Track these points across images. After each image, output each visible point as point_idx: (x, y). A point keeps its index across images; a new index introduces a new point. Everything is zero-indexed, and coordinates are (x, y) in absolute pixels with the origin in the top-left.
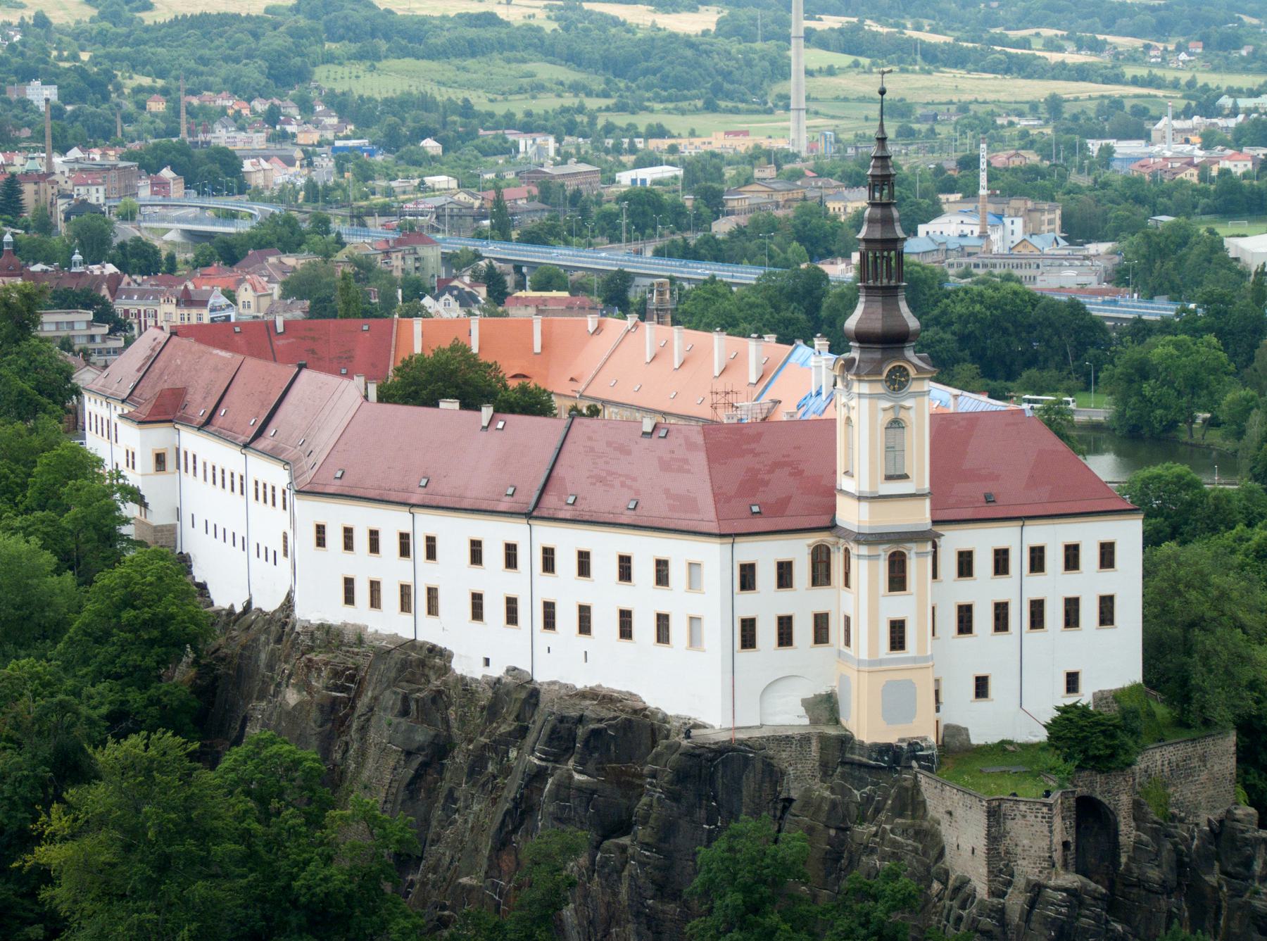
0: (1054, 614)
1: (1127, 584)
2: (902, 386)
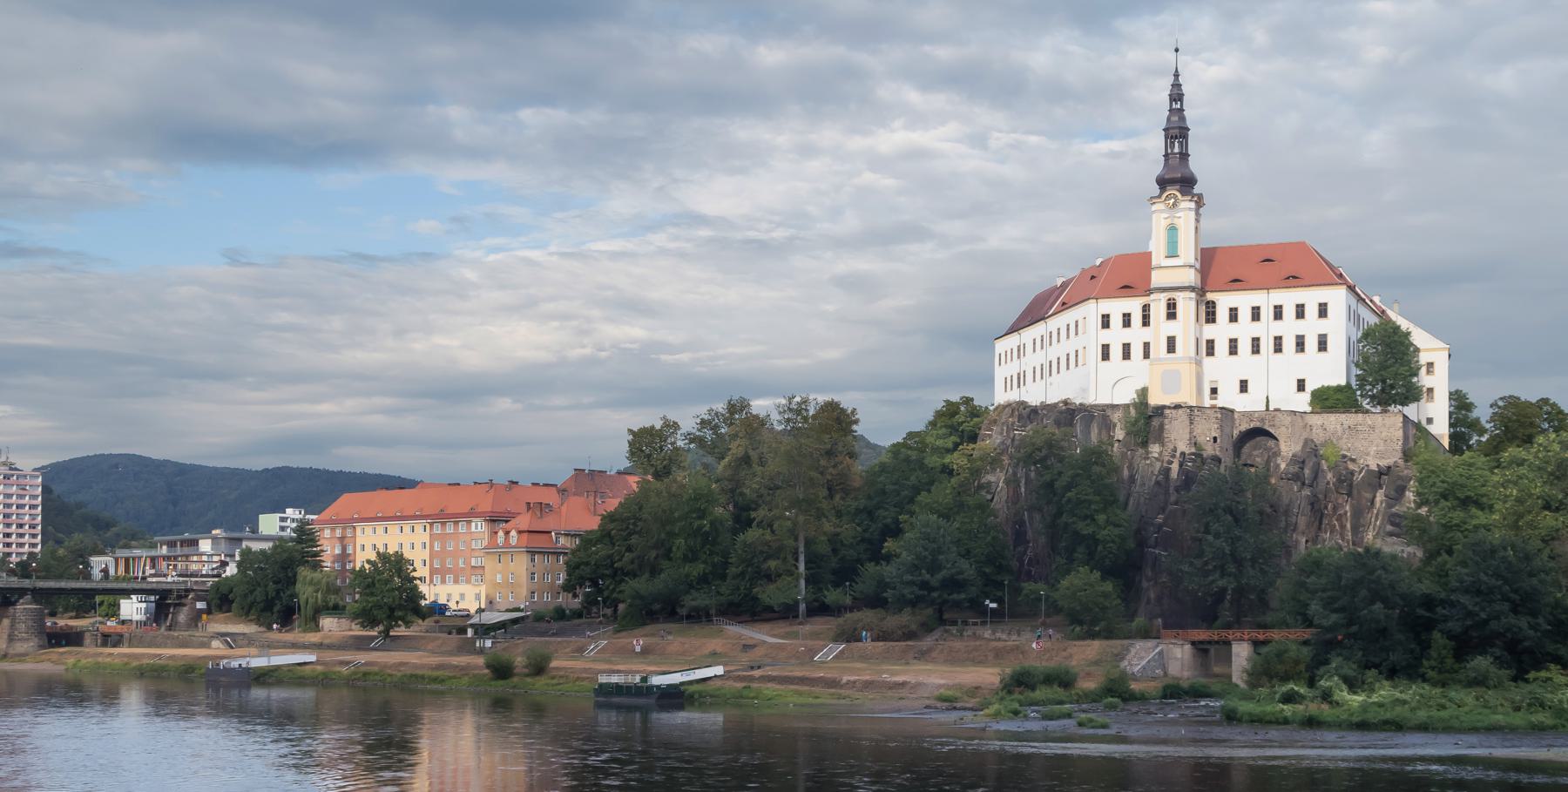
0: (1289, 344)
1: (1338, 328)
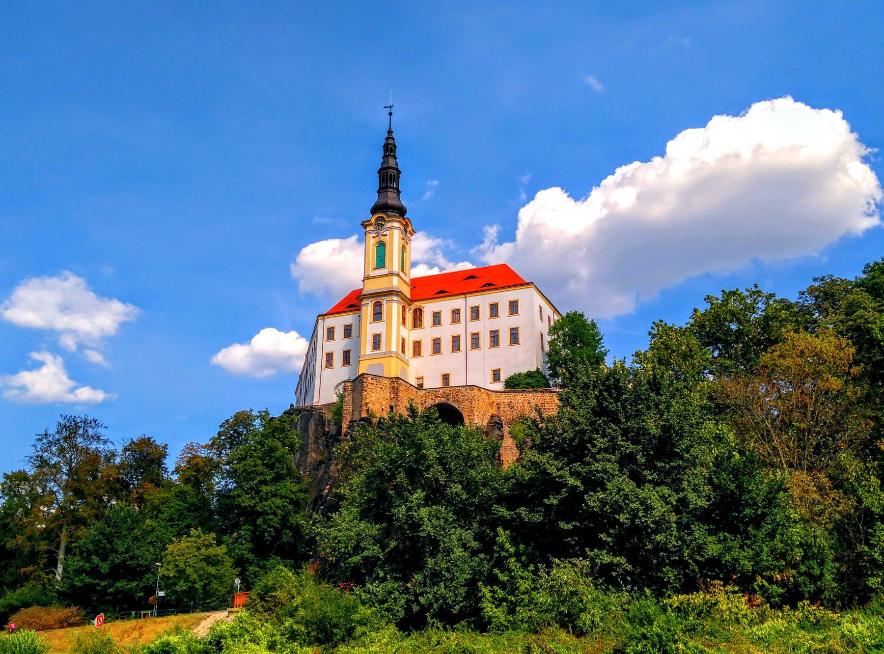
2: (382, 225)
